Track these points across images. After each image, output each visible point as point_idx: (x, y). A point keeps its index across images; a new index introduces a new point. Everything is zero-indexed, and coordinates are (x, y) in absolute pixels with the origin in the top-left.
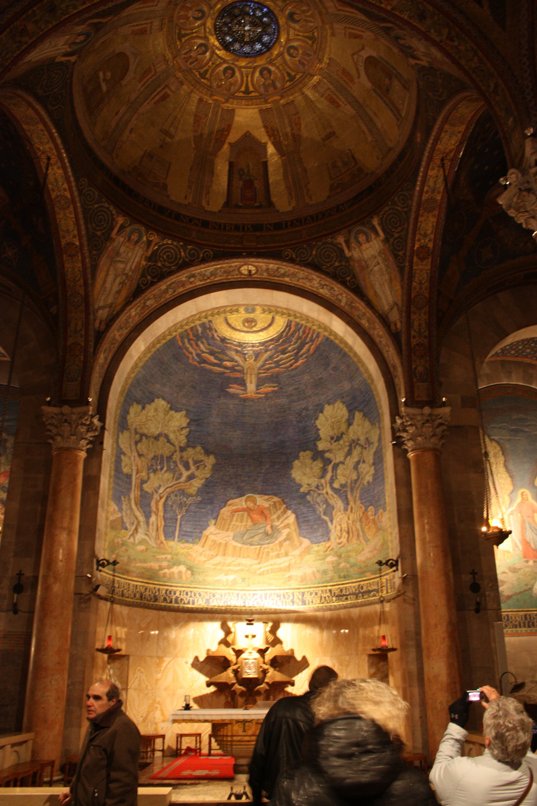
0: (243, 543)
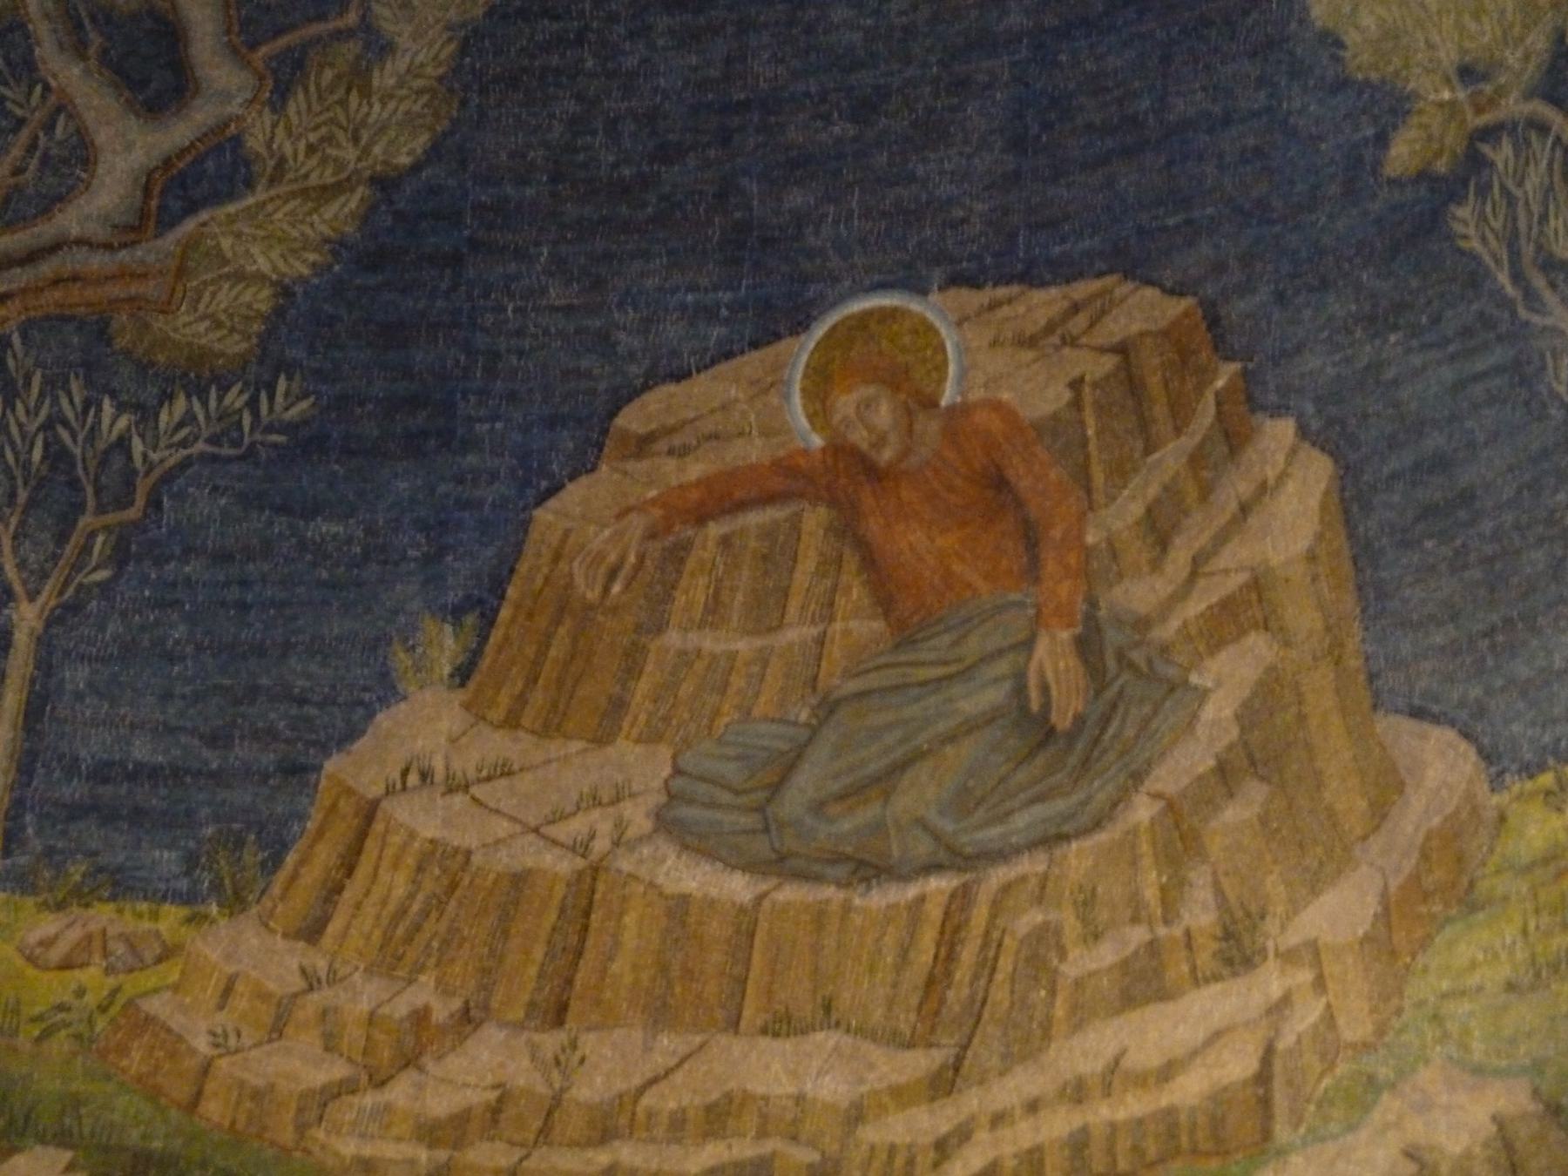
0: (780, 866)
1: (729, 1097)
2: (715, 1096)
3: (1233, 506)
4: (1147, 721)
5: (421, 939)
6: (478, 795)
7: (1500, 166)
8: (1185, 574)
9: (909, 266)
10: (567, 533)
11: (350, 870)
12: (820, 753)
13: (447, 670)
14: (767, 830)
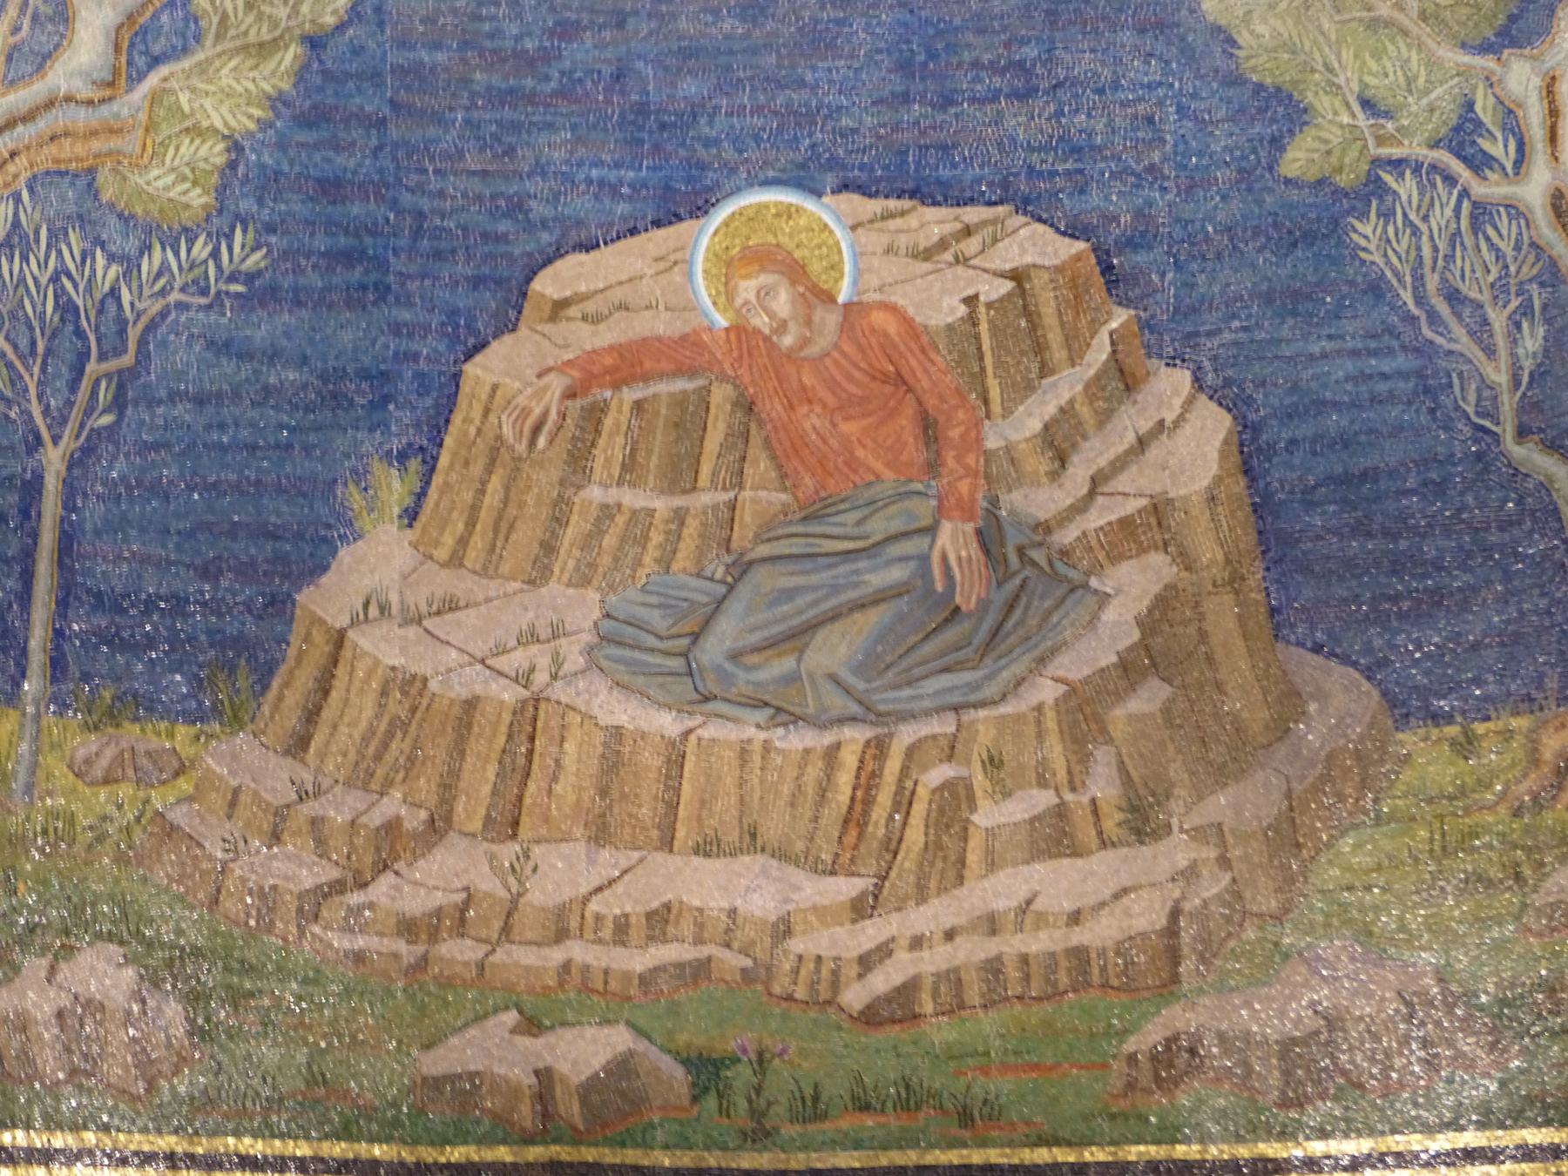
1: (667, 907)
2: (655, 904)
3: (1130, 438)
4: (1049, 613)
5: (389, 758)
6: (430, 628)
7: (1404, 198)
8: (1085, 490)
9: (803, 166)
10: (495, 388)
11: (326, 693)
12: (735, 607)
13: (396, 511)
14: (690, 674)
